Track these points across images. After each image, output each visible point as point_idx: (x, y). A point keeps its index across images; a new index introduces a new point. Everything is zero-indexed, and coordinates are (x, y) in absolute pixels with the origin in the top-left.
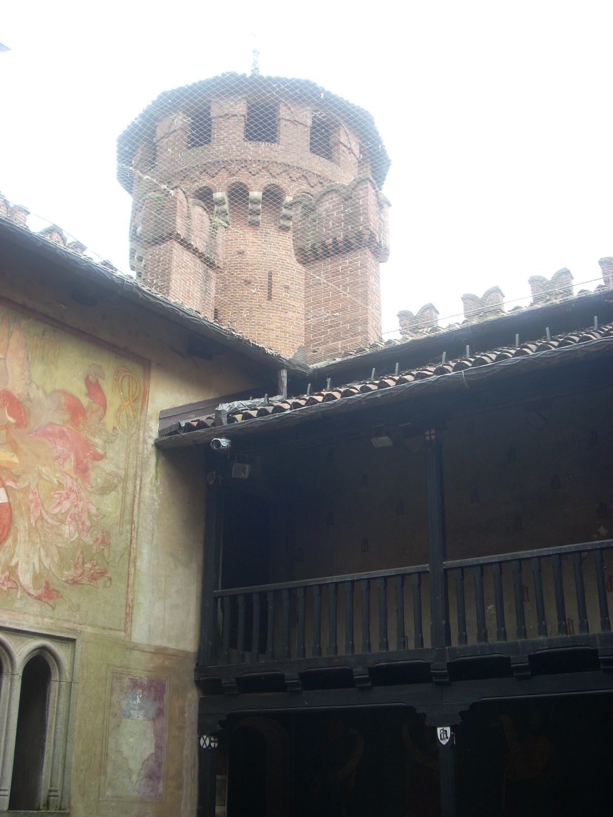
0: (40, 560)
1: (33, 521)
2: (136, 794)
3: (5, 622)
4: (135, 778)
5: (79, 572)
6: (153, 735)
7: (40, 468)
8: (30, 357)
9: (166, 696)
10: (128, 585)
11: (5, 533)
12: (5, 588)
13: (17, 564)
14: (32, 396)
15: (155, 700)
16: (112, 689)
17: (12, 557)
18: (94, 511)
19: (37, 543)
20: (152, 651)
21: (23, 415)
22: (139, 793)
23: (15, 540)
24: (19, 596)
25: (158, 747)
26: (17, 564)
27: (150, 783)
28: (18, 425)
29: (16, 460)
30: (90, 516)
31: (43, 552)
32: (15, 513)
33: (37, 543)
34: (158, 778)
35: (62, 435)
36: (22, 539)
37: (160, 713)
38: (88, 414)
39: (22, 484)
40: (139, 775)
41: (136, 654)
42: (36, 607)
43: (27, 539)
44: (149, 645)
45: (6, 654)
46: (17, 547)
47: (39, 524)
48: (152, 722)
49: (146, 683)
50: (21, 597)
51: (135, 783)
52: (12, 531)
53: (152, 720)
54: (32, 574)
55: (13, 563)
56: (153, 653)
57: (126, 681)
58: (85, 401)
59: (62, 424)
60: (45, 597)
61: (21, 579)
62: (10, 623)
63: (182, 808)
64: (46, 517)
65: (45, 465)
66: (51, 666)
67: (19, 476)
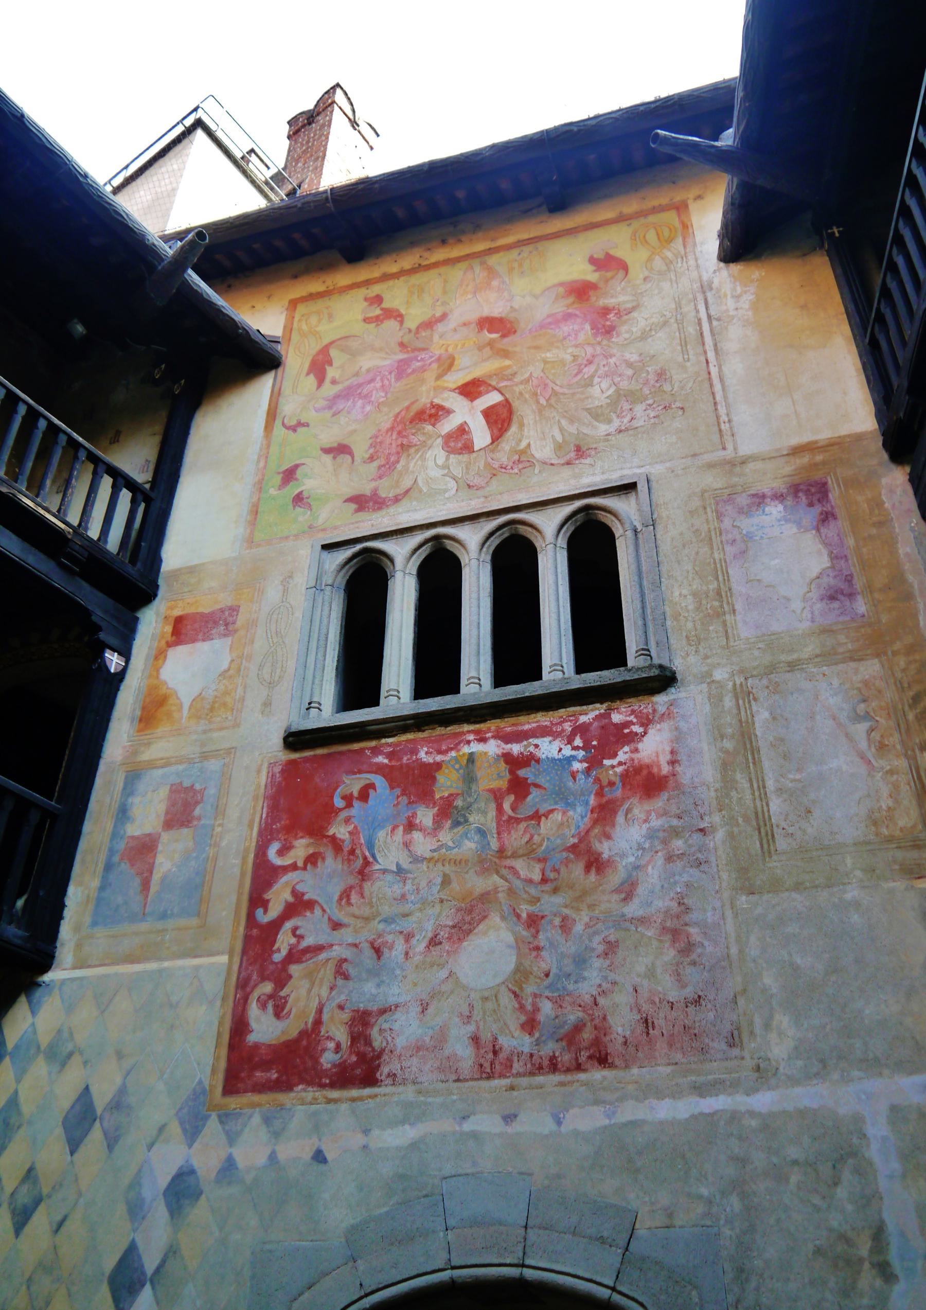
0: (561, 430)
1: (543, 401)
2: (806, 625)
3: (520, 501)
4: (797, 605)
5: (626, 420)
6: (820, 546)
7: (543, 355)
8: (507, 280)
9: (834, 495)
10: (715, 404)
11: (506, 425)
12: (516, 471)
13: (529, 445)
14: (517, 307)
15: (811, 505)
16: (720, 516)
17: (520, 441)
18: (634, 358)
19: (554, 417)
20: (785, 453)
21: (508, 325)
22: (813, 621)
23: (521, 425)
24: (536, 471)
25: (834, 557)
26: (529, 445)
27: (836, 604)
28: (504, 336)
29: (507, 362)
30: (629, 365)
31: (564, 422)
32: (516, 404)
33: (554, 417)
34: (851, 596)
35: (567, 317)
36: (531, 422)
37: (827, 517)
38: (601, 285)
39: (518, 379)
40: (805, 599)
41: (751, 466)
42: (566, 472)
43: (538, 418)
44: (777, 450)
45: (534, 531)
46: (526, 430)
47: (552, 401)
48: (814, 532)
49: (785, 491)
50: (540, 472)
51: (799, 612)
52: (515, 419)
53: (813, 529)
54: (552, 446)
55: (523, 445)
56: (787, 455)
57: (743, 500)
58: (592, 276)
59: (566, 308)
60: (576, 459)
61: (538, 455)
62: (528, 499)
63: (922, 623)
64: (557, 388)
65: (549, 350)
66: (610, 525)
67: (516, 373)
